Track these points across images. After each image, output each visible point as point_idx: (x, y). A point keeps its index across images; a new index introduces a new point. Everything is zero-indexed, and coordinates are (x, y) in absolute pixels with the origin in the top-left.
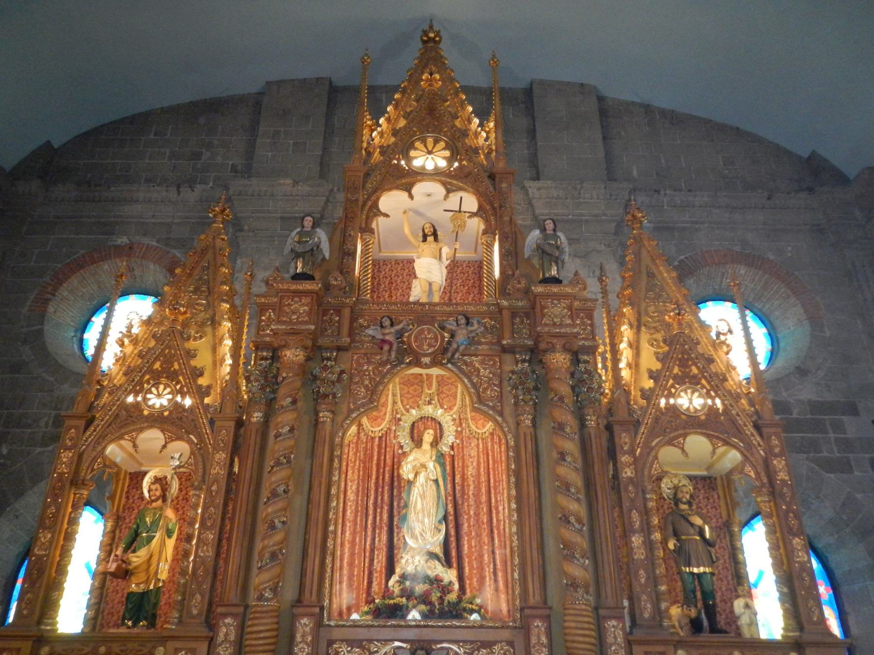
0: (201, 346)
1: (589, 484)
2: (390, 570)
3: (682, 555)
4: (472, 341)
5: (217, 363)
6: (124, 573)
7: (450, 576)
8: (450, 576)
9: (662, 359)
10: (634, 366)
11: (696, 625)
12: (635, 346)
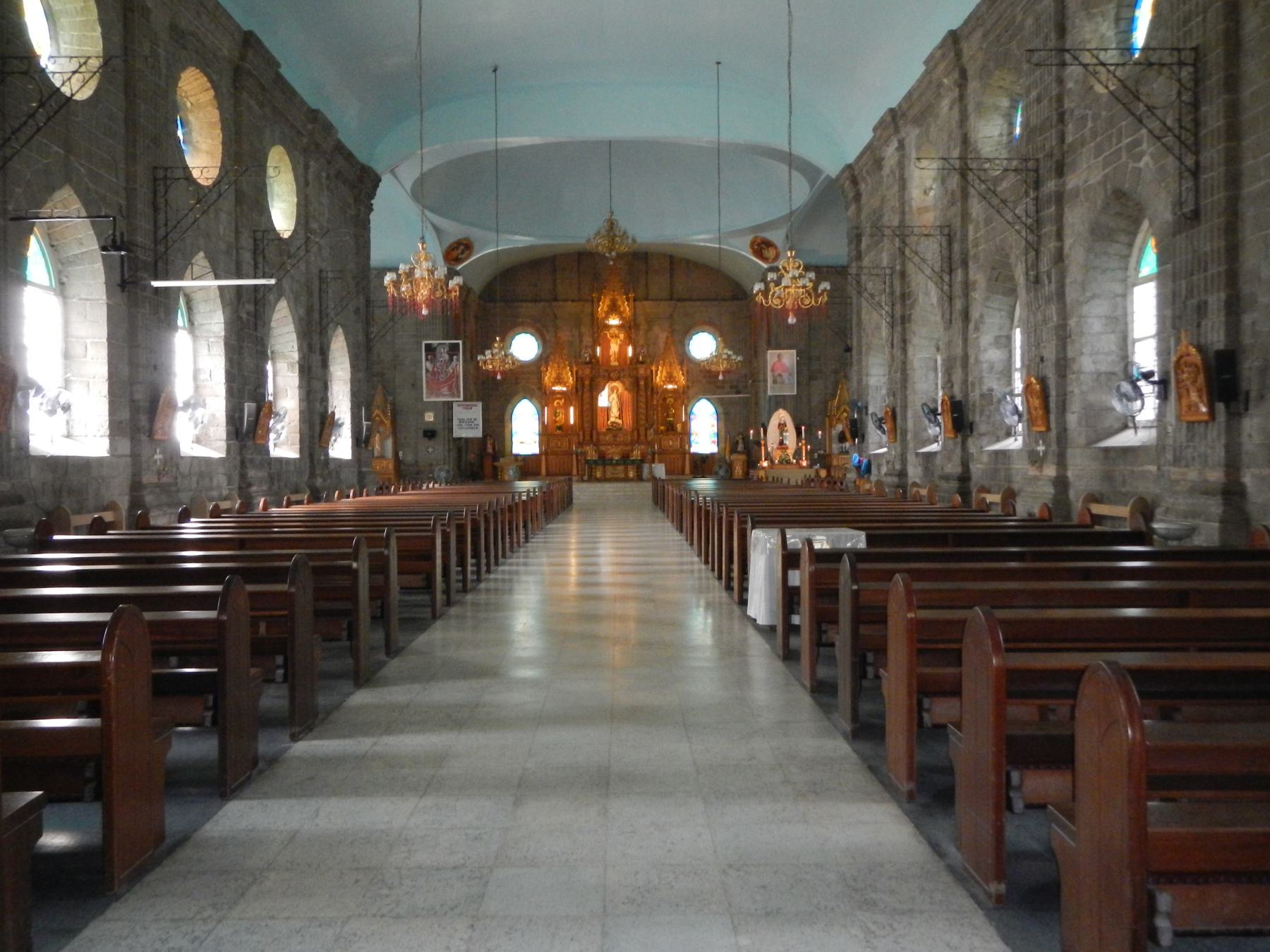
0: (564, 375)
1: (647, 407)
2: (608, 420)
3: (668, 416)
4: (624, 375)
5: (568, 378)
6: (556, 422)
7: (620, 421)
8: (620, 421)
9: (665, 377)
10: (661, 377)
11: (668, 430)
12: (662, 372)
